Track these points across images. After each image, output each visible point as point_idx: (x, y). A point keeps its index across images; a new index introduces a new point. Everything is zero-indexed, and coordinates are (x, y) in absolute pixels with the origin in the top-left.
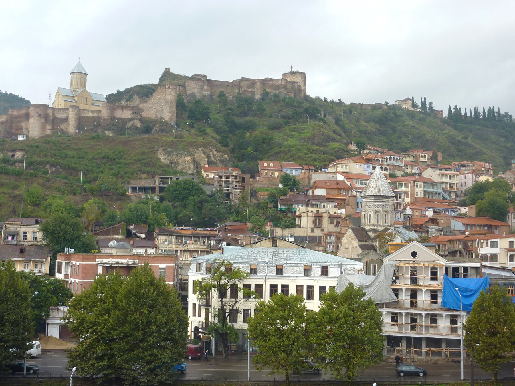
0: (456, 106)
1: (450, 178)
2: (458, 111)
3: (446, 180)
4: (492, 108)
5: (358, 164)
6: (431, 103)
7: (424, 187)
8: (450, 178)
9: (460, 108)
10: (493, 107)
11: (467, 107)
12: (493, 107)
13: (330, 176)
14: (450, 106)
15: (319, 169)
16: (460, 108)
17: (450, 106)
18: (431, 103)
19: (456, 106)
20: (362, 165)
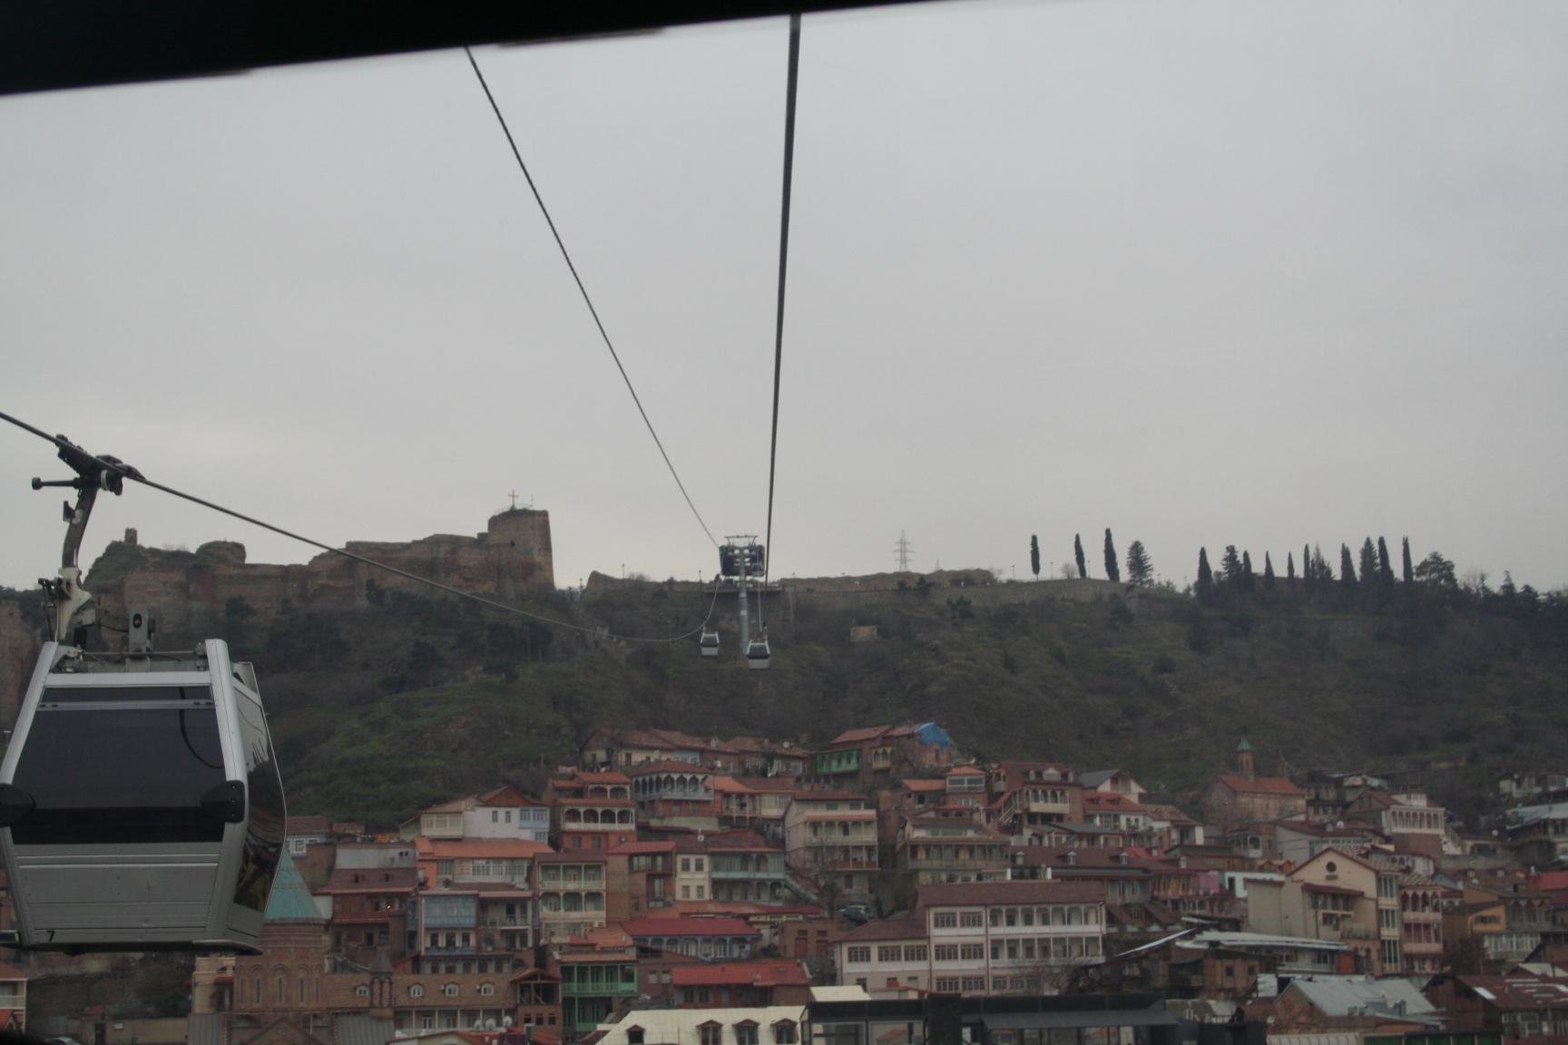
0: (1231, 550)
1: (846, 832)
2: (1238, 567)
3: (837, 837)
4: (1376, 547)
5: (502, 812)
6: (1136, 549)
7: (716, 868)
8: (846, 832)
9: (1246, 555)
10: (1381, 541)
11: (1276, 549)
12: (1381, 541)
13: (394, 852)
14: (1203, 553)
15: (375, 831)
16: (1246, 555)
17: (1203, 553)
18: (1136, 549)
19: (1231, 550)
20: (515, 813)
